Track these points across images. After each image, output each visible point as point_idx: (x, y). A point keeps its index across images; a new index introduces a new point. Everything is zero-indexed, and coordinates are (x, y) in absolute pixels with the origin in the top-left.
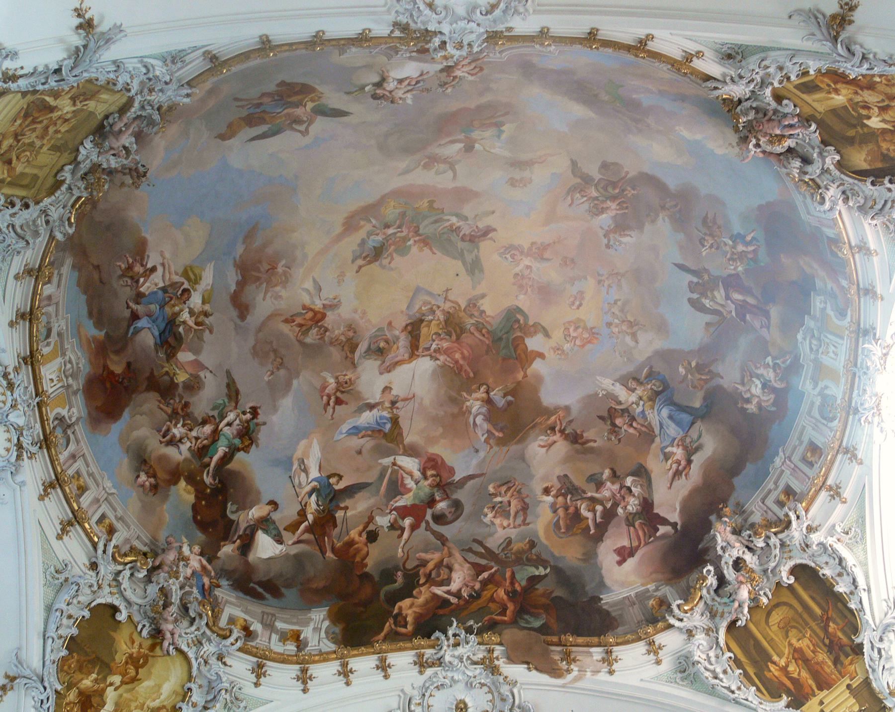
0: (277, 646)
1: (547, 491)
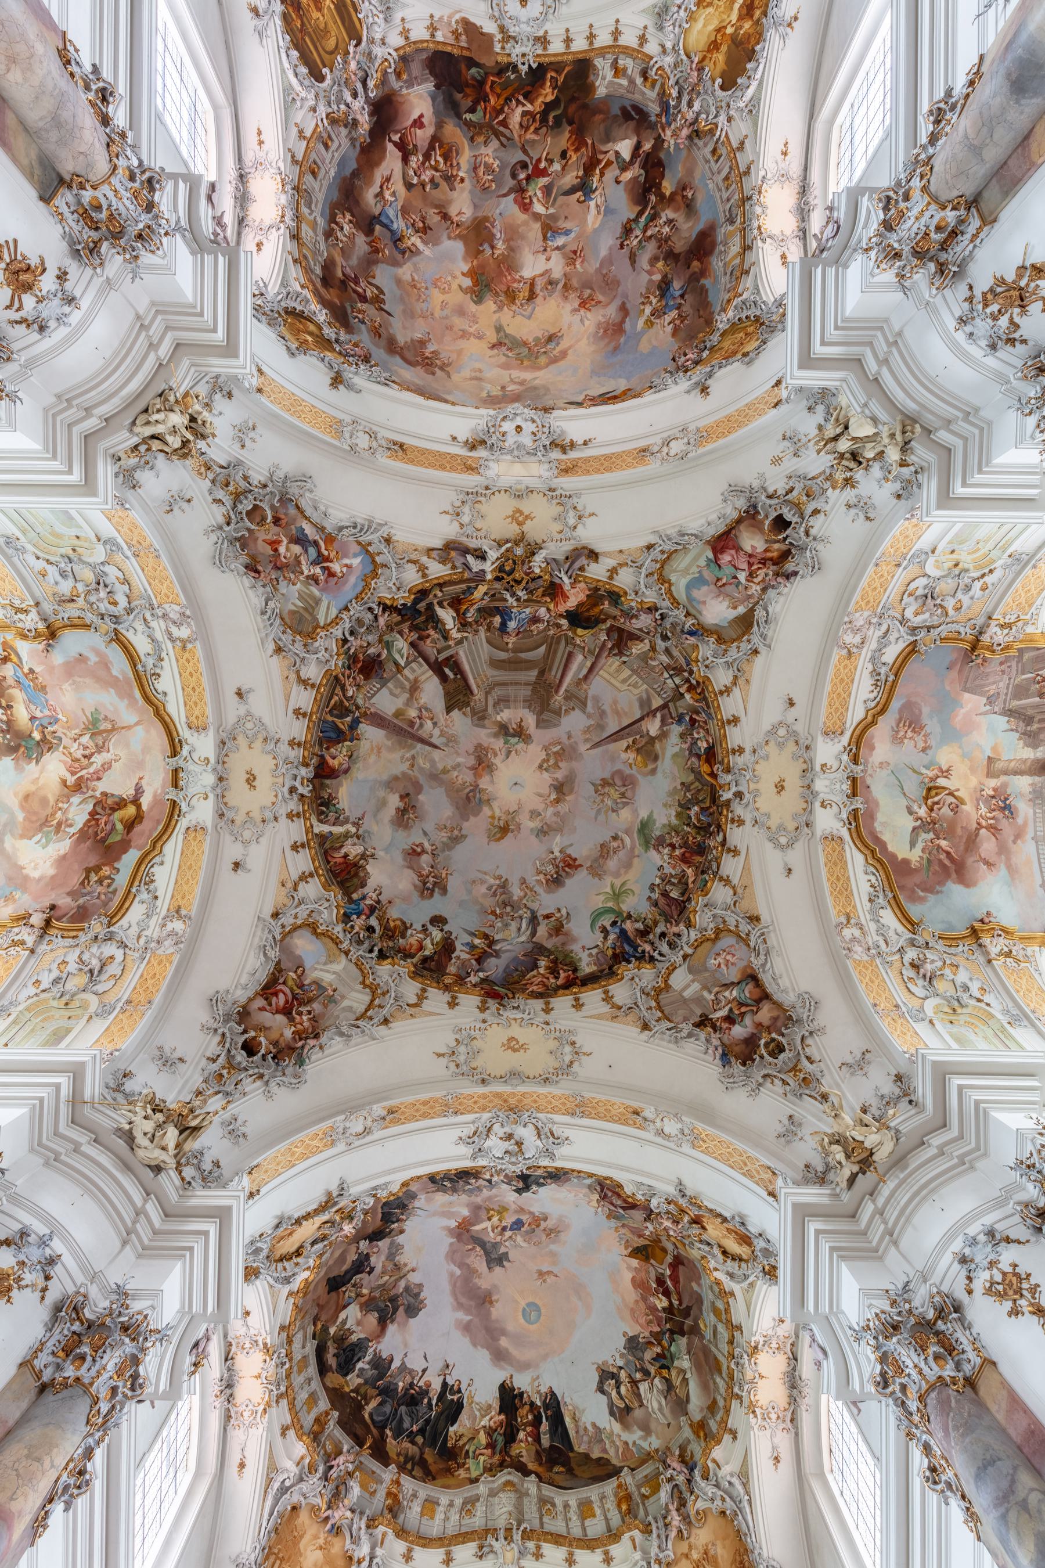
1: (462, 180)
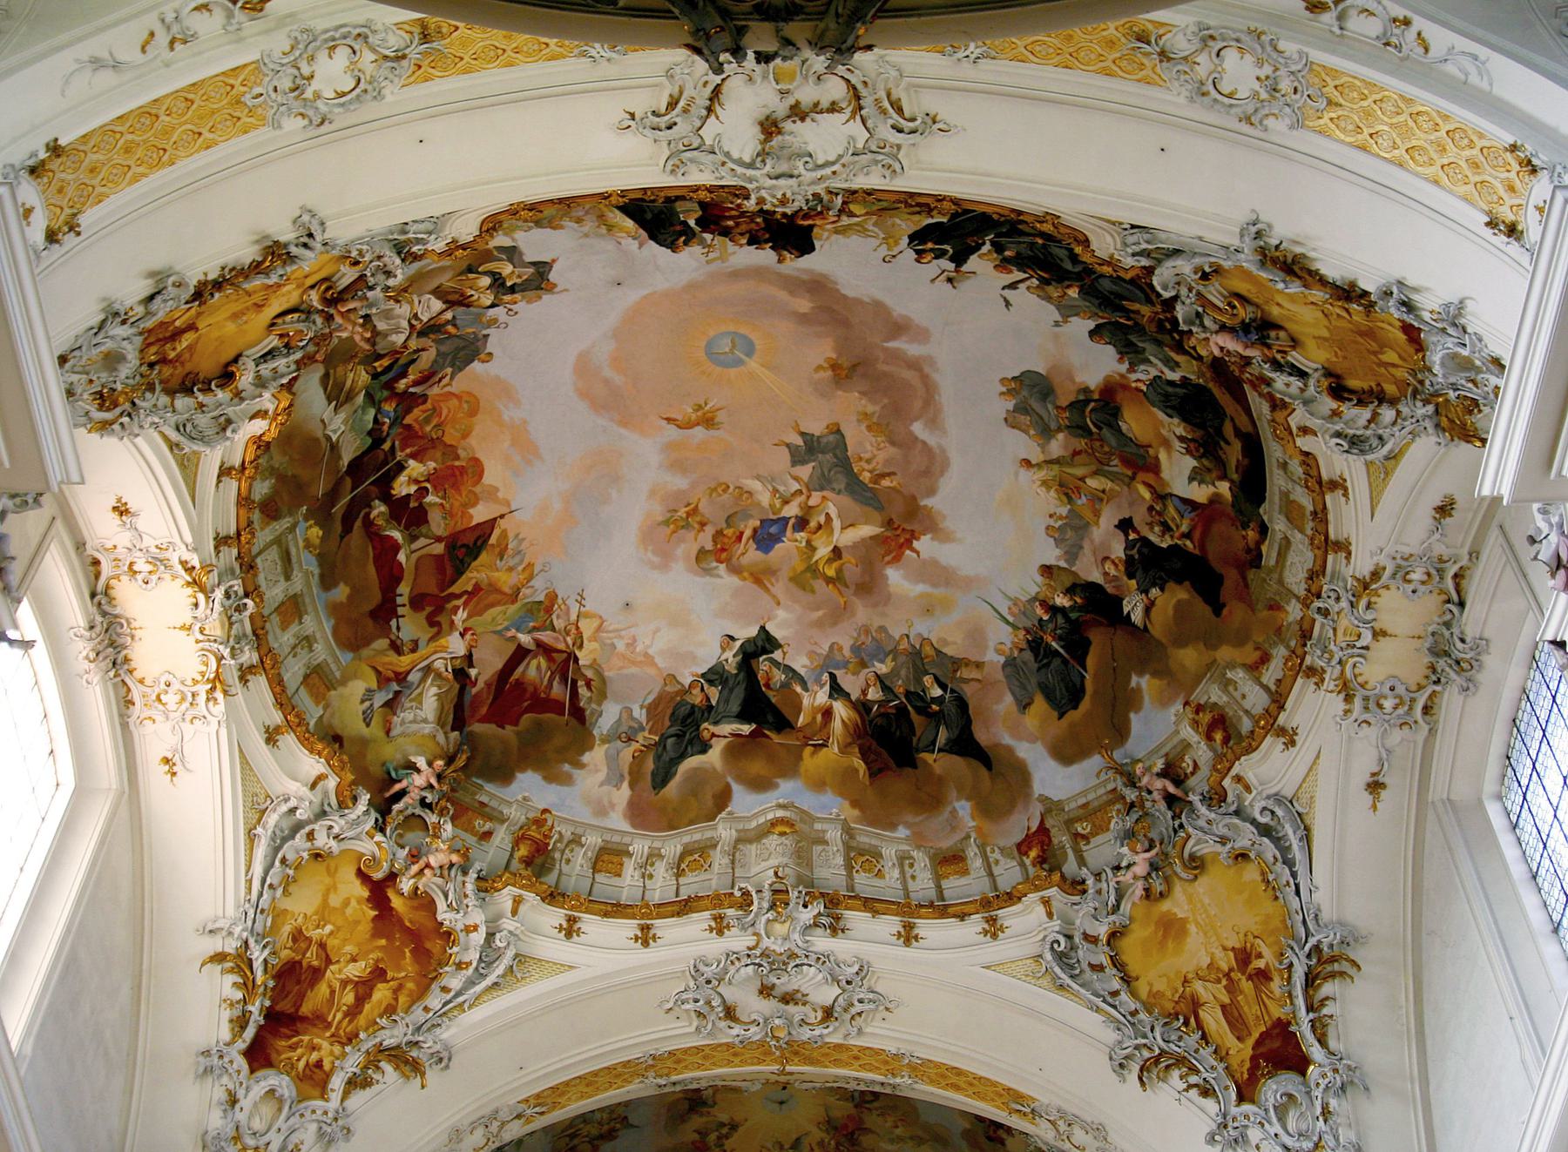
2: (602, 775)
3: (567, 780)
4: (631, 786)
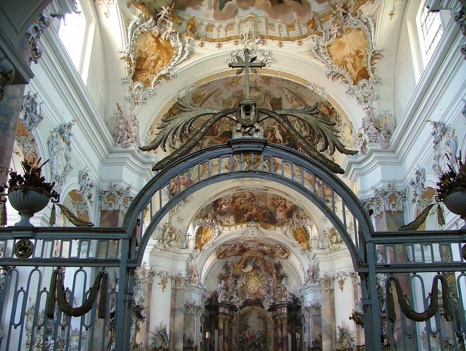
0: (226, 224)
1: (270, 199)
2: (207, 7)
3: (198, 9)
4: (214, 9)
